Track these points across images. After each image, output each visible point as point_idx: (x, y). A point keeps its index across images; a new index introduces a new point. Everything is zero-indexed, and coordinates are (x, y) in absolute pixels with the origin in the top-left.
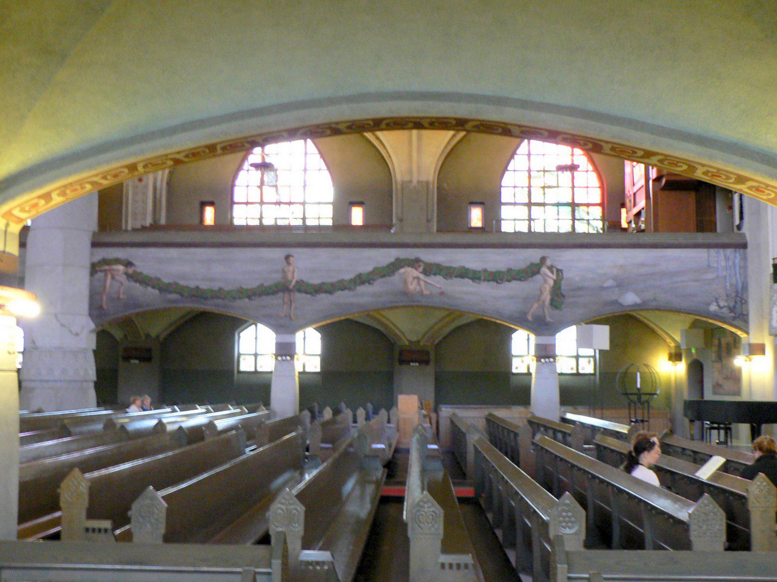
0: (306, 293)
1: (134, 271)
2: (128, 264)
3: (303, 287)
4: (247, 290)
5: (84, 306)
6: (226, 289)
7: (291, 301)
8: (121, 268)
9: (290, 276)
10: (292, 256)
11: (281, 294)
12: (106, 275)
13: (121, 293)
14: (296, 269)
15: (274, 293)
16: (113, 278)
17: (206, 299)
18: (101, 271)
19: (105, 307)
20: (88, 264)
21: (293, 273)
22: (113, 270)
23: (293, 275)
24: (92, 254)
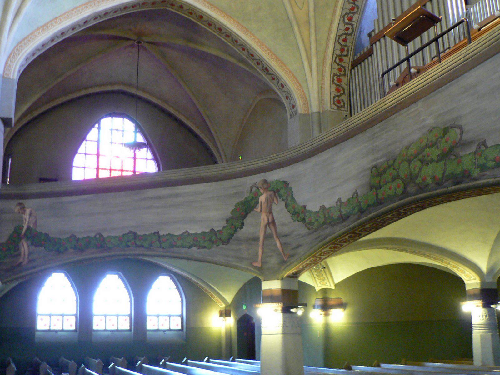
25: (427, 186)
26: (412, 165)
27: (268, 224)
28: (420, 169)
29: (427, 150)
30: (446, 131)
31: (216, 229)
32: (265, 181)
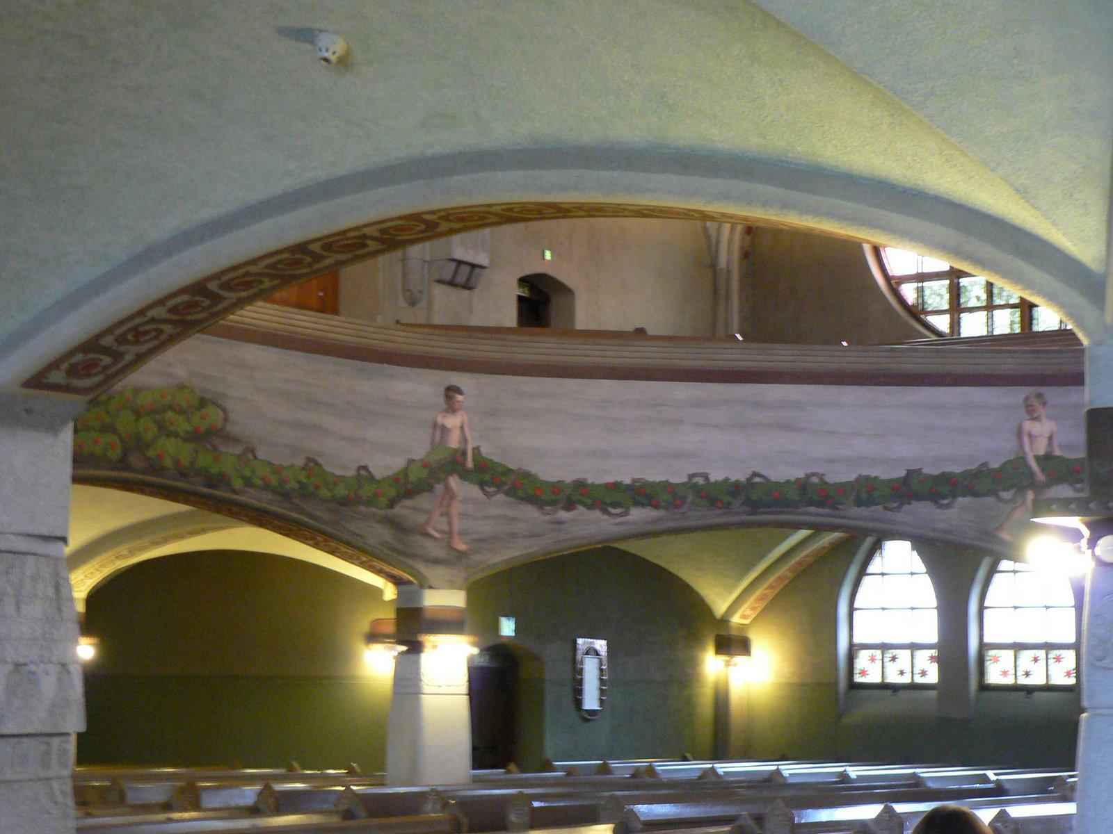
25: (163, 468)
26: (142, 422)
28: (155, 438)
29: (170, 415)
30: (203, 403)
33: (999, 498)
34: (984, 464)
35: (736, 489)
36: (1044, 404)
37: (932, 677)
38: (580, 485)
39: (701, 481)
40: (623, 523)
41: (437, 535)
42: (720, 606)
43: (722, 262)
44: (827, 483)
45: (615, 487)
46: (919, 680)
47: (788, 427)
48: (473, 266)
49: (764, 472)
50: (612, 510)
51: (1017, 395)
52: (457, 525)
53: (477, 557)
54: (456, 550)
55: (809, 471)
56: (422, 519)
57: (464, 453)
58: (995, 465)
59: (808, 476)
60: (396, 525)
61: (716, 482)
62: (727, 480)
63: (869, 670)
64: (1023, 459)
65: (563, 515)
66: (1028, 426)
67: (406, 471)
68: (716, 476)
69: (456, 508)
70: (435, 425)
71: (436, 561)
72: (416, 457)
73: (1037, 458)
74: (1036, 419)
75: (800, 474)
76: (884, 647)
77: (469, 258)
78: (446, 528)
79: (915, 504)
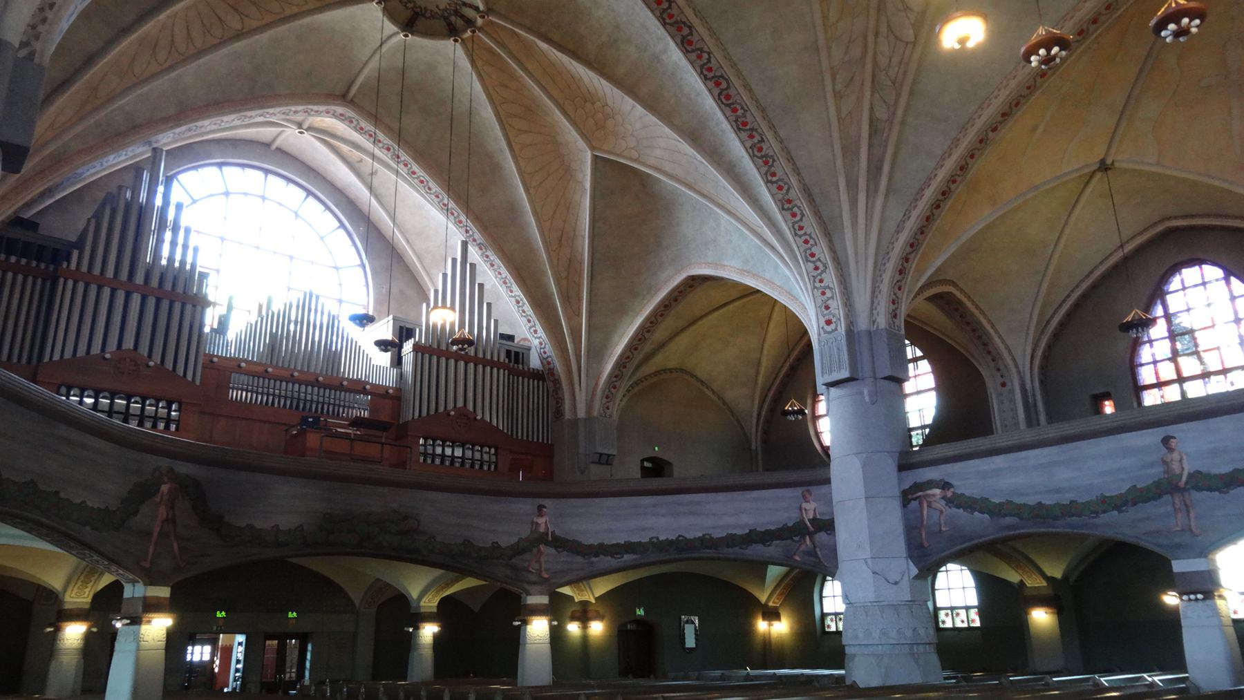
0: (1210, 490)
1: (954, 493)
2: (945, 485)
3: (1201, 481)
4: (1111, 497)
5: (900, 546)
6: (1080, 501)
7: (1187, 506)
8: (937, 491)
9: (1176, 467)
10: (1175, 438)
11: (1167, 497)
12: (921, 504)
13: (943, 525)
14: (1185, 457)
15: (1159, 496)
16: (929, 506)
17: (1055, 518)
18: (915, 499)
19: (926, 545)
20: (897, 493)
21: (1181, 461)
22: (928, 495)
23: (1182, 465)
24: (900, 481)
27: (166, 520)
31: (111, 509)
32: (171, 470)
33: (793, 541)
34: (786, 524)
35: (670, 543)
36: (811, 495)
37: (977, 624)
38: (601, 545)
39: (655, 540)
40: (621, 562)
41: (534, 571)
42: (763, 599)
43: (753, 447)
44: (713, 538)
45: (618, 545)
46: (972, 625)
47: (691, 513)
48: (609, 455)
49: (683, 535)
50: (615, 556)
51: (798, 491)
52: (543, 566)
53: (554, 581)
54: (542, 577)
55: (704, 533)
56: (526, 564)
57: (547, 534)
58: (790, 524)
59: (704, 535)
60: (515, 568)
61: (662, 540)
62: (667, 539)
63: (947, 622)
64: (803, 521)
65: (594, 559)
66: (804, 505)
67: (517, 544)
68: (662, 538)
69: (543, 559)
70: (532, 522)
71: (535, 583)
72: (523, 537)
73: (809, 520)
74: (809, 502)
75: (700, 535)
76: (952, 609)
77: (606, 451)
78: (537, 567)
79: (754, 545)
